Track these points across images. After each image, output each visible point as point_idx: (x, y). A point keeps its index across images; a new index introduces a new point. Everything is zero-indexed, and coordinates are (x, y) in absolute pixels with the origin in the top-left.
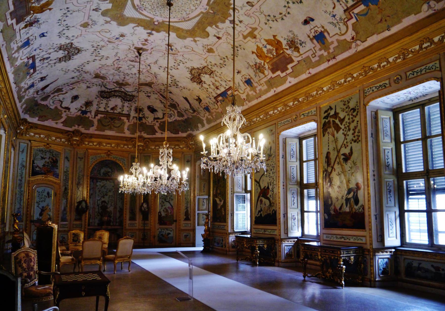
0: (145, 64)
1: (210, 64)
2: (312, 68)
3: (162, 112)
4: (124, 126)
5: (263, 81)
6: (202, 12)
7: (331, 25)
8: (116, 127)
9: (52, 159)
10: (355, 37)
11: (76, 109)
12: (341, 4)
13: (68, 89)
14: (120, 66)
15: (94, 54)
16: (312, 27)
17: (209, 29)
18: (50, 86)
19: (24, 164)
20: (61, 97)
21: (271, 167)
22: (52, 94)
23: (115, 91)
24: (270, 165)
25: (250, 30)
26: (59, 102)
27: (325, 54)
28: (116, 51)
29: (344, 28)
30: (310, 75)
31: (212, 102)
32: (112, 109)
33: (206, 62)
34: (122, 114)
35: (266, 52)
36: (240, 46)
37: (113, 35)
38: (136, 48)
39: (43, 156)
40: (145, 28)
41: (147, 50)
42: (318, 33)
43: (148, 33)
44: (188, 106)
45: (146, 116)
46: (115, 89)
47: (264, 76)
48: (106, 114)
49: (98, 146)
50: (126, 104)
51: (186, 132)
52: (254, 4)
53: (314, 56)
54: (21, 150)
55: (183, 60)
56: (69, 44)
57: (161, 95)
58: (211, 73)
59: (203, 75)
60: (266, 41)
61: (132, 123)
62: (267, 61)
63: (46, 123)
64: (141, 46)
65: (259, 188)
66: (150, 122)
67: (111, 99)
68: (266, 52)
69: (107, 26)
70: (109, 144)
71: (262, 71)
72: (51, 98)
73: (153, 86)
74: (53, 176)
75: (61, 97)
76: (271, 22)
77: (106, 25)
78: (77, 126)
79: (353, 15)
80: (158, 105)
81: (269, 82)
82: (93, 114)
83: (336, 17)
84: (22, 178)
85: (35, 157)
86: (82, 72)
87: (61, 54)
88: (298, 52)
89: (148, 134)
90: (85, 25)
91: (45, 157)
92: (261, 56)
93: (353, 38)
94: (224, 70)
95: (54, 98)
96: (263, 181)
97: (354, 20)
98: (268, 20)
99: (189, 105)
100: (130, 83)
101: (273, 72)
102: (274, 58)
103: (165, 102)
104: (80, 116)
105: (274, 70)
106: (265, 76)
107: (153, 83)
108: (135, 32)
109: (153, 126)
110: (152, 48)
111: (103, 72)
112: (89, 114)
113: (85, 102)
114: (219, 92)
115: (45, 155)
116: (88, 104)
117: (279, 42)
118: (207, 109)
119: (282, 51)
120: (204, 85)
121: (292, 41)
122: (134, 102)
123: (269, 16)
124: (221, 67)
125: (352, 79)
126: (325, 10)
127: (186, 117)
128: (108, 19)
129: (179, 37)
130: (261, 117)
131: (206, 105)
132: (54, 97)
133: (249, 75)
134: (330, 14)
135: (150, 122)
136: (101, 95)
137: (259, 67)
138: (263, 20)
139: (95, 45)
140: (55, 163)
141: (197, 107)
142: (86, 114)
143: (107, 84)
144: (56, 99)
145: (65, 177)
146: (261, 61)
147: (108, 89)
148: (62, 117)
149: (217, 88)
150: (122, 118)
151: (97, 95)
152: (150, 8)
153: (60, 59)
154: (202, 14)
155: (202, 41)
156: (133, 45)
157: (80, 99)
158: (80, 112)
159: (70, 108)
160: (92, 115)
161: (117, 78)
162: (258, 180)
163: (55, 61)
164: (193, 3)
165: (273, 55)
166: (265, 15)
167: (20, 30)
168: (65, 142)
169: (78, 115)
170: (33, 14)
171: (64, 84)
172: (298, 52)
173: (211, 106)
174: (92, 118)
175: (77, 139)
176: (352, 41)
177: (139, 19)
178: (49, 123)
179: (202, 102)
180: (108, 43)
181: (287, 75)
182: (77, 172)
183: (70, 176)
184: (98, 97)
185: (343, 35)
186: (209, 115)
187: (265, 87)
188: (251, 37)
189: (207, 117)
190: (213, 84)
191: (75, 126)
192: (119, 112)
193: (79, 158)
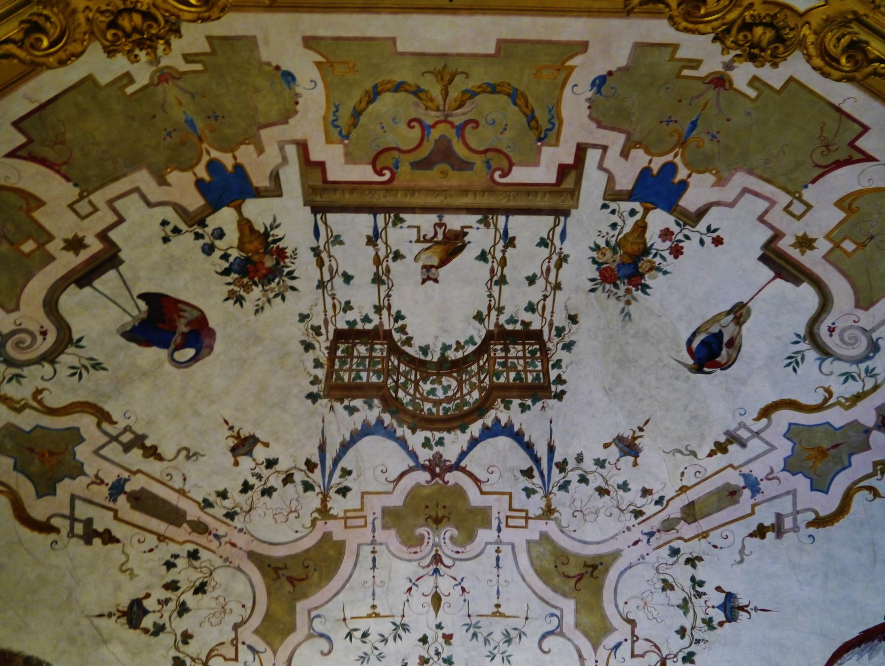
3: (92, 350)
8: (399, 87)
11: (718, 241)
26: (832, 342)
45: (186, 243)
48: (492, 188)
57: (174, 516)
66: (131, 207)
67: (479, 333)
72: (876, 387)
89: (89, 81)
95: (854, 388)
103: (113, 451)
104: (695, 167)
112: (626, 181)
113: (645, 288)
122: (317, 330)
132: (858, 398)
135: (131, 207)
144: (848, 377)
148: (846, 203)
150: (364, 173)
151: (568, 347)
158: (690, 201)
159: (763, 259)
160: (601, 167)
169: (710, 178)
174: (605, 148)
184: (560, 331)
192: (398, 221)
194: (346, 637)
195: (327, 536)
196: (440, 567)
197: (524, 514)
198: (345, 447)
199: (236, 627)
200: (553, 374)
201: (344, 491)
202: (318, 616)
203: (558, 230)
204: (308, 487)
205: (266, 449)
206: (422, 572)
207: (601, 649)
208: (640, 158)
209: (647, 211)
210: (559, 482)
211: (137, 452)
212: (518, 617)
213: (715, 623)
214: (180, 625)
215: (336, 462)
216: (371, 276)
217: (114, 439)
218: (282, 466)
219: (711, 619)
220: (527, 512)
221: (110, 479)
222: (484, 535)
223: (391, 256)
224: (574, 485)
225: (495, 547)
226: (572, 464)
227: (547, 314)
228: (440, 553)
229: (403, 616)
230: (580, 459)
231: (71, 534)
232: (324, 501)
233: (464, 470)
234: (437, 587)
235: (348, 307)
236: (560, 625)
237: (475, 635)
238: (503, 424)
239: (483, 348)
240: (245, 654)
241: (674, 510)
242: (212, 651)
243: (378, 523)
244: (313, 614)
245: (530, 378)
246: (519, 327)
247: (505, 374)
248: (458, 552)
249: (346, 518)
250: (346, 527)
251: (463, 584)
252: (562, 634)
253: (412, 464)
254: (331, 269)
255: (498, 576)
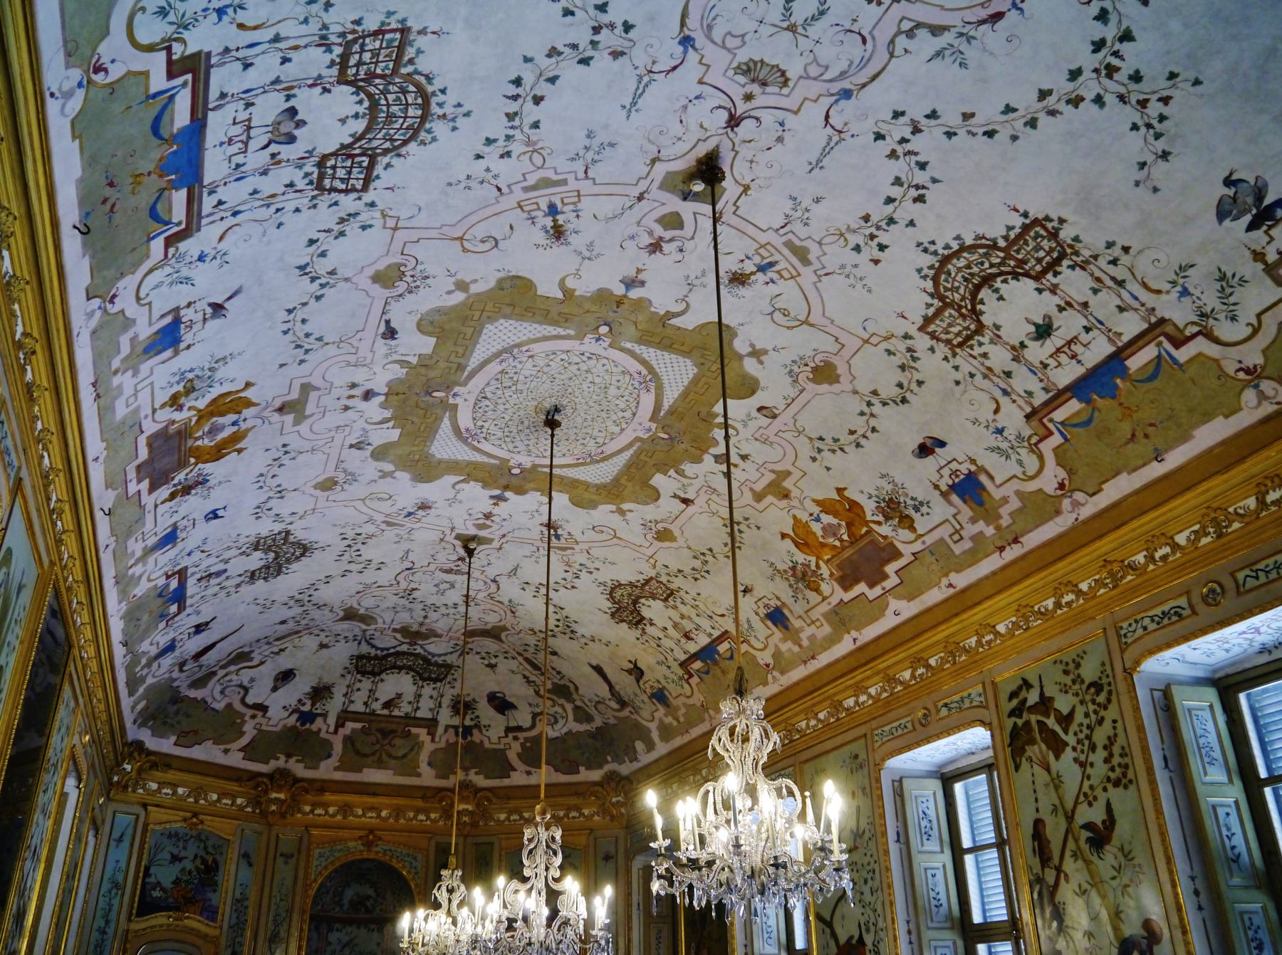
0: (482, 577)
1: (665, 571)
2: (957, 572)
3: (529, 709)
4: (418, 754)
5: (816, 614)
6: (638, 439)
7: (995, 456)
8: (396, 758)
9: (204, 861)
10: (1066, 482)
12: (1014, 401)
13: (266, 653)
14: (413, 586)
15: (347, 557)
16: (943, 463)
17: (658, 480)
18: (218, 646)
19: (120, 878)
20: (245, 676)
21: (864, 874)
22: (223, 667)
23: (398, 654)
24: (859, 866)
25: (773, 476)
26: (238, 689)
27: (990, 531)
28: (405, 546)
29: (1032, 463)
30: (951, 591)
31: (672, 676)
32: (388, 705)
33: (654, 567)
34: (415, 718)
35: (819, 533)
36: (747, 519)
37: (399, 505)
38: (458, 537)
39: (175, 851)
40: (486, 485)
41: (489, 541)
42: (962, 477)
43: (492, 497)
44: (604, 691)
45: (484, 722)
46: (398, 649)
47: (820, 598)
48: (370, 722)
49: (339, 817)
50: (428, 690)
51: (600, 767)
52: (777, 412)
53: (956, 537)
54: (116, 835)
55: (589, 564)
56: (280, 533)
57: (527, 660)
58: (669, 596)
59: (647, 603)
60: (818, 503)
61: (443, 745)
62: (826, 558)
63: (197, 753)
64: (472, 531)
65: (832, 944)
66: (494, 739)
67: (384, 676)
68: (819, 533)
69: (385, 486)
70: (372, 809)
71: (812, 585)
73: (503, 635)
74: (201, 915)
75: (245, 676)
76: (826, 454)
77: (382, 481)
78: (283, 758)
79: (1051, 426)
80: (517, 690)
81: (837, 614)
82: (332, 720)
83: (1005, 434)
84: (107, 922)
85: (155, 855)
86: (308, 606)
87: (256, 560)
88: (912, 528)
89: (487, 777)
90: (328, 485)
91: (183, 854)
92: (806, 544)
93: (1061, 486)
94: (705, 587)
95: (228, 678)
96: (843, 917)
97: (1056, 439)
98: (820, 451)
99: (607, 688)
100: (439, 632)
101: (846, 588)
102: (843, 548)
103: (538, 682)
104: (294, 727)
105: (846, 582)
106: (824, 599)
107: (504, 629)
108: (459, 496)
109: (503, 752)
110: (504, 536)
111: (368, 602)
112: (319, 721)
114: (693, 648)
115: (185, 848)
116: (320, 692)
117: (854, 505)
118: (660, 696)
119: (864, 530)
120: (649, 629)
121: (891, 499)
123: (821, 439)
124: (696, 579)
125: (1077, 599)
126: (972, 416)
127: (598, 722)
128: (389, 467)
129: (577, 502)
130: (821, 716)
131: (656, 685)
132: (226, 675)
133: (778, 598)
134: (987, 427)
135: (494, 739)
136: (357, 667)
137: (804, 574)
138: (806, 450)
139: (350, 534)
140: (209, 872)
141: (630, 691)
142: (312, 722)
143: (377, 634)
145: (235, 915)
146: (809, 558)
147: (377, 649)
148: (242, 734)
149: (687, 636)
150: (414, 730)
152: (500, 434)
153: (253, 573)
154: (638, 444)
155: (640, 513)
156: (453, 529)
157: (297, 679)
158: (295, 716)
161: (404, 618)
162: (827, 917)
163: (239, 580)
164: (614, 417)
165: (841, 541)
166: (810, 439)
167: (156, 506)
168: (246, 806)
170: (196, 464)
171: (258, 641)
172: (912, 528)
173: (673, 690)
175: (282, 796)
176: (1059, 492)
177: (469, 463)
178: (206, 752)
179: (645, 678)
180: (383, 526)
181: (886, 592)
182: (273, 901)
183: (251, 912)
185: (1032, 478)
186: (666, 715)
187: (827, 629)
188: (775, 496)
189: (661, 720)
190: (676, 626)
191: (278, 759)
193: (282, 855)
208: (314, 727)
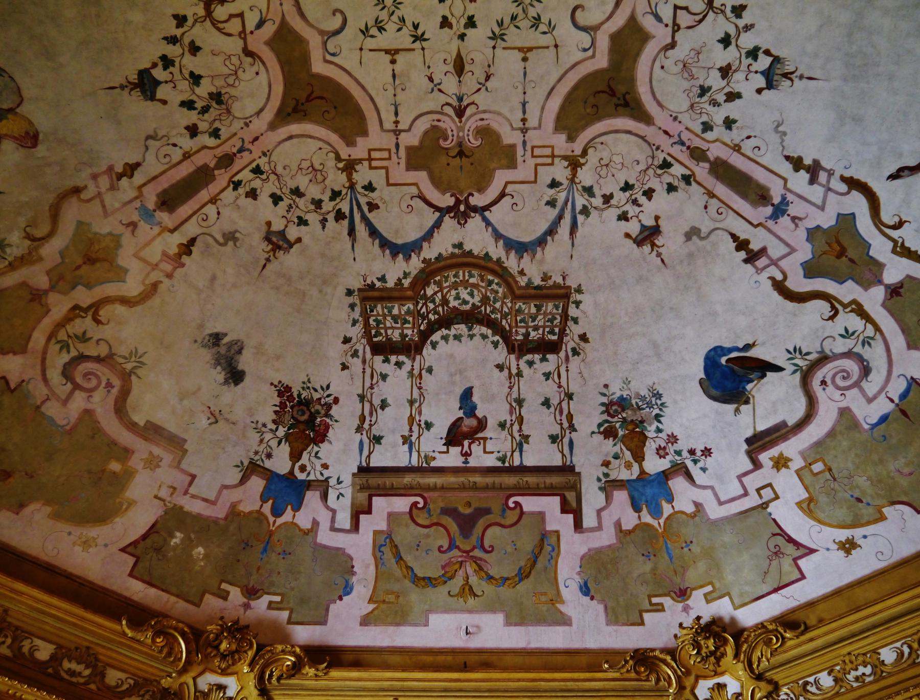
78: (236, 594)
112: (312, 498)
150: (530, 504)
151: (346, 340)
158: (257, 484)
174: (333, 529)
192: (502, 459)
194: (555, 26)
195: (571, 139)
196: (455, 103)
197: (374, 164)
198: (551, 231)
199: (672, 45)
200: (357, 314)
201: (554, 184)
202: (585, 50)
203: (366, 452)
204: (589, 191)
205: (628, 231)
206: (477, 98)
207: (278, 20)
208: (303, 519)
209: (291, 472)
210: (342, 199)
211: (755, 246)
212: (371, 50)
213: (160, 64)
214: (729, 55)
215: (560, 217)
216: (525, 404)
217: (775, 263)
218: (613, 213)
219: (165, 68)
220: (371, 168)
221: (785, 220)
222: (412, 139)
223: (508, 425)
224: (326, 198)
225: (400, 127)
226: (331, 217)
227: (368, 371)
228: (457, 120)
229: (494, 47)
230: (324, 221)
231: (831, 173)
232: (574, 175)
233: (437, 209)
234: (460, 82)
235: (547, 376)
236: (325, 43)
237: (416, 27)
238: (401, 256)
239: (425, 336)
240: (666, 13)
241: (222, 178)
242: (700, 21)
243: (520, 151)
244: (590, 53)
245: (379, 307)
246: (393, 359)
247: (403, 313)
248: (439, 121)
249: (553, 156)
250: (553, 147)
251: (431, 85)
252: (322, 33)
253: (487, 213)
254: (561, 413)
255: (395, 95)
